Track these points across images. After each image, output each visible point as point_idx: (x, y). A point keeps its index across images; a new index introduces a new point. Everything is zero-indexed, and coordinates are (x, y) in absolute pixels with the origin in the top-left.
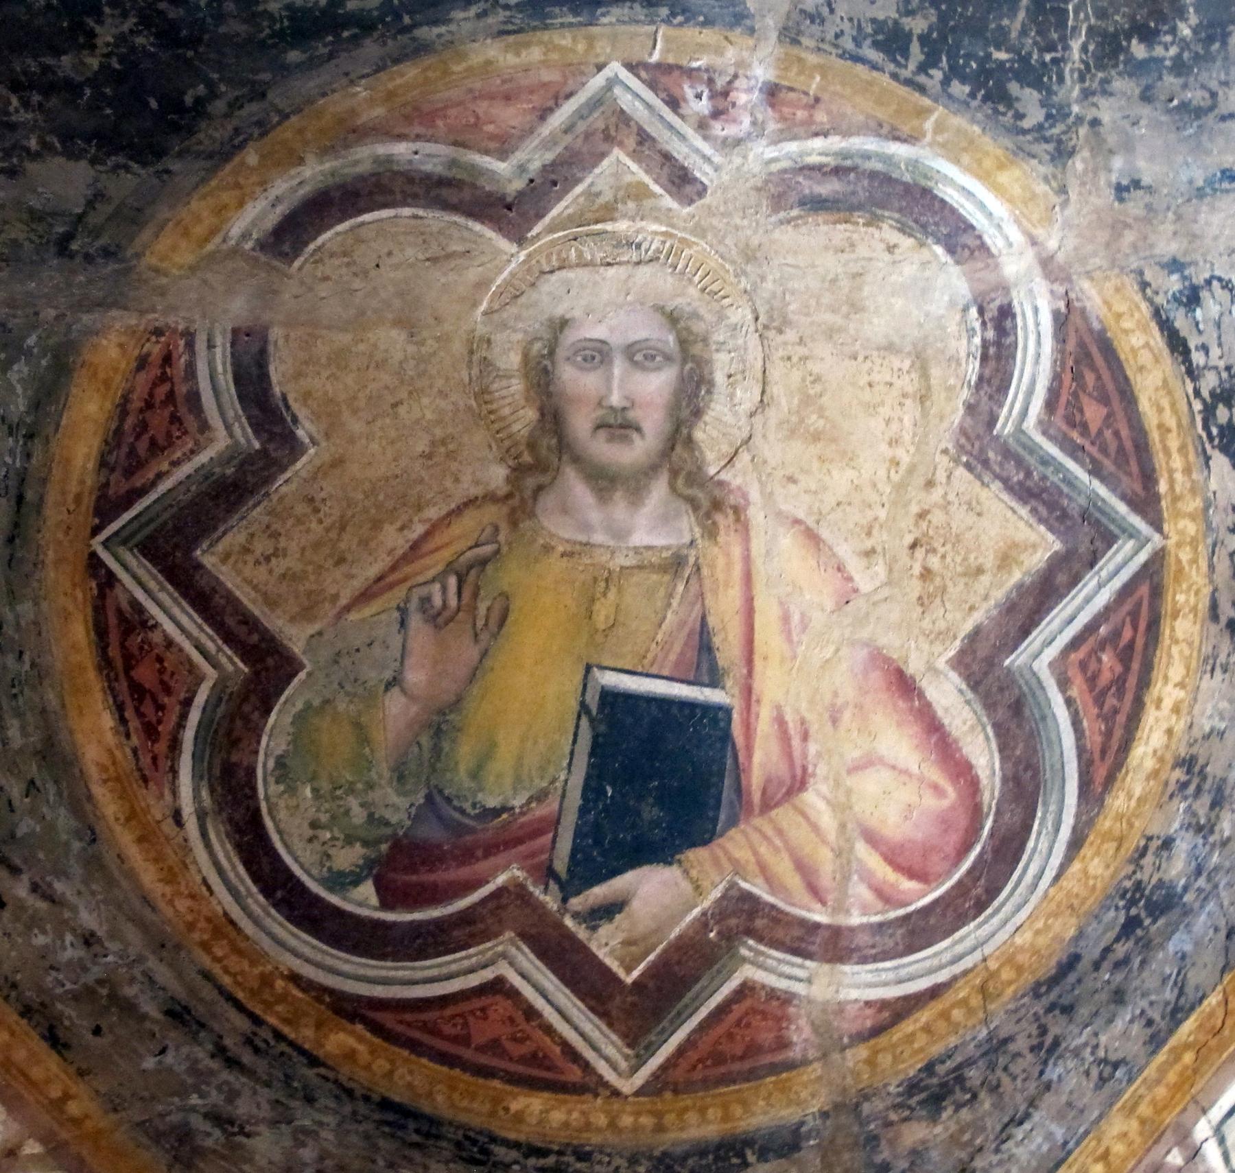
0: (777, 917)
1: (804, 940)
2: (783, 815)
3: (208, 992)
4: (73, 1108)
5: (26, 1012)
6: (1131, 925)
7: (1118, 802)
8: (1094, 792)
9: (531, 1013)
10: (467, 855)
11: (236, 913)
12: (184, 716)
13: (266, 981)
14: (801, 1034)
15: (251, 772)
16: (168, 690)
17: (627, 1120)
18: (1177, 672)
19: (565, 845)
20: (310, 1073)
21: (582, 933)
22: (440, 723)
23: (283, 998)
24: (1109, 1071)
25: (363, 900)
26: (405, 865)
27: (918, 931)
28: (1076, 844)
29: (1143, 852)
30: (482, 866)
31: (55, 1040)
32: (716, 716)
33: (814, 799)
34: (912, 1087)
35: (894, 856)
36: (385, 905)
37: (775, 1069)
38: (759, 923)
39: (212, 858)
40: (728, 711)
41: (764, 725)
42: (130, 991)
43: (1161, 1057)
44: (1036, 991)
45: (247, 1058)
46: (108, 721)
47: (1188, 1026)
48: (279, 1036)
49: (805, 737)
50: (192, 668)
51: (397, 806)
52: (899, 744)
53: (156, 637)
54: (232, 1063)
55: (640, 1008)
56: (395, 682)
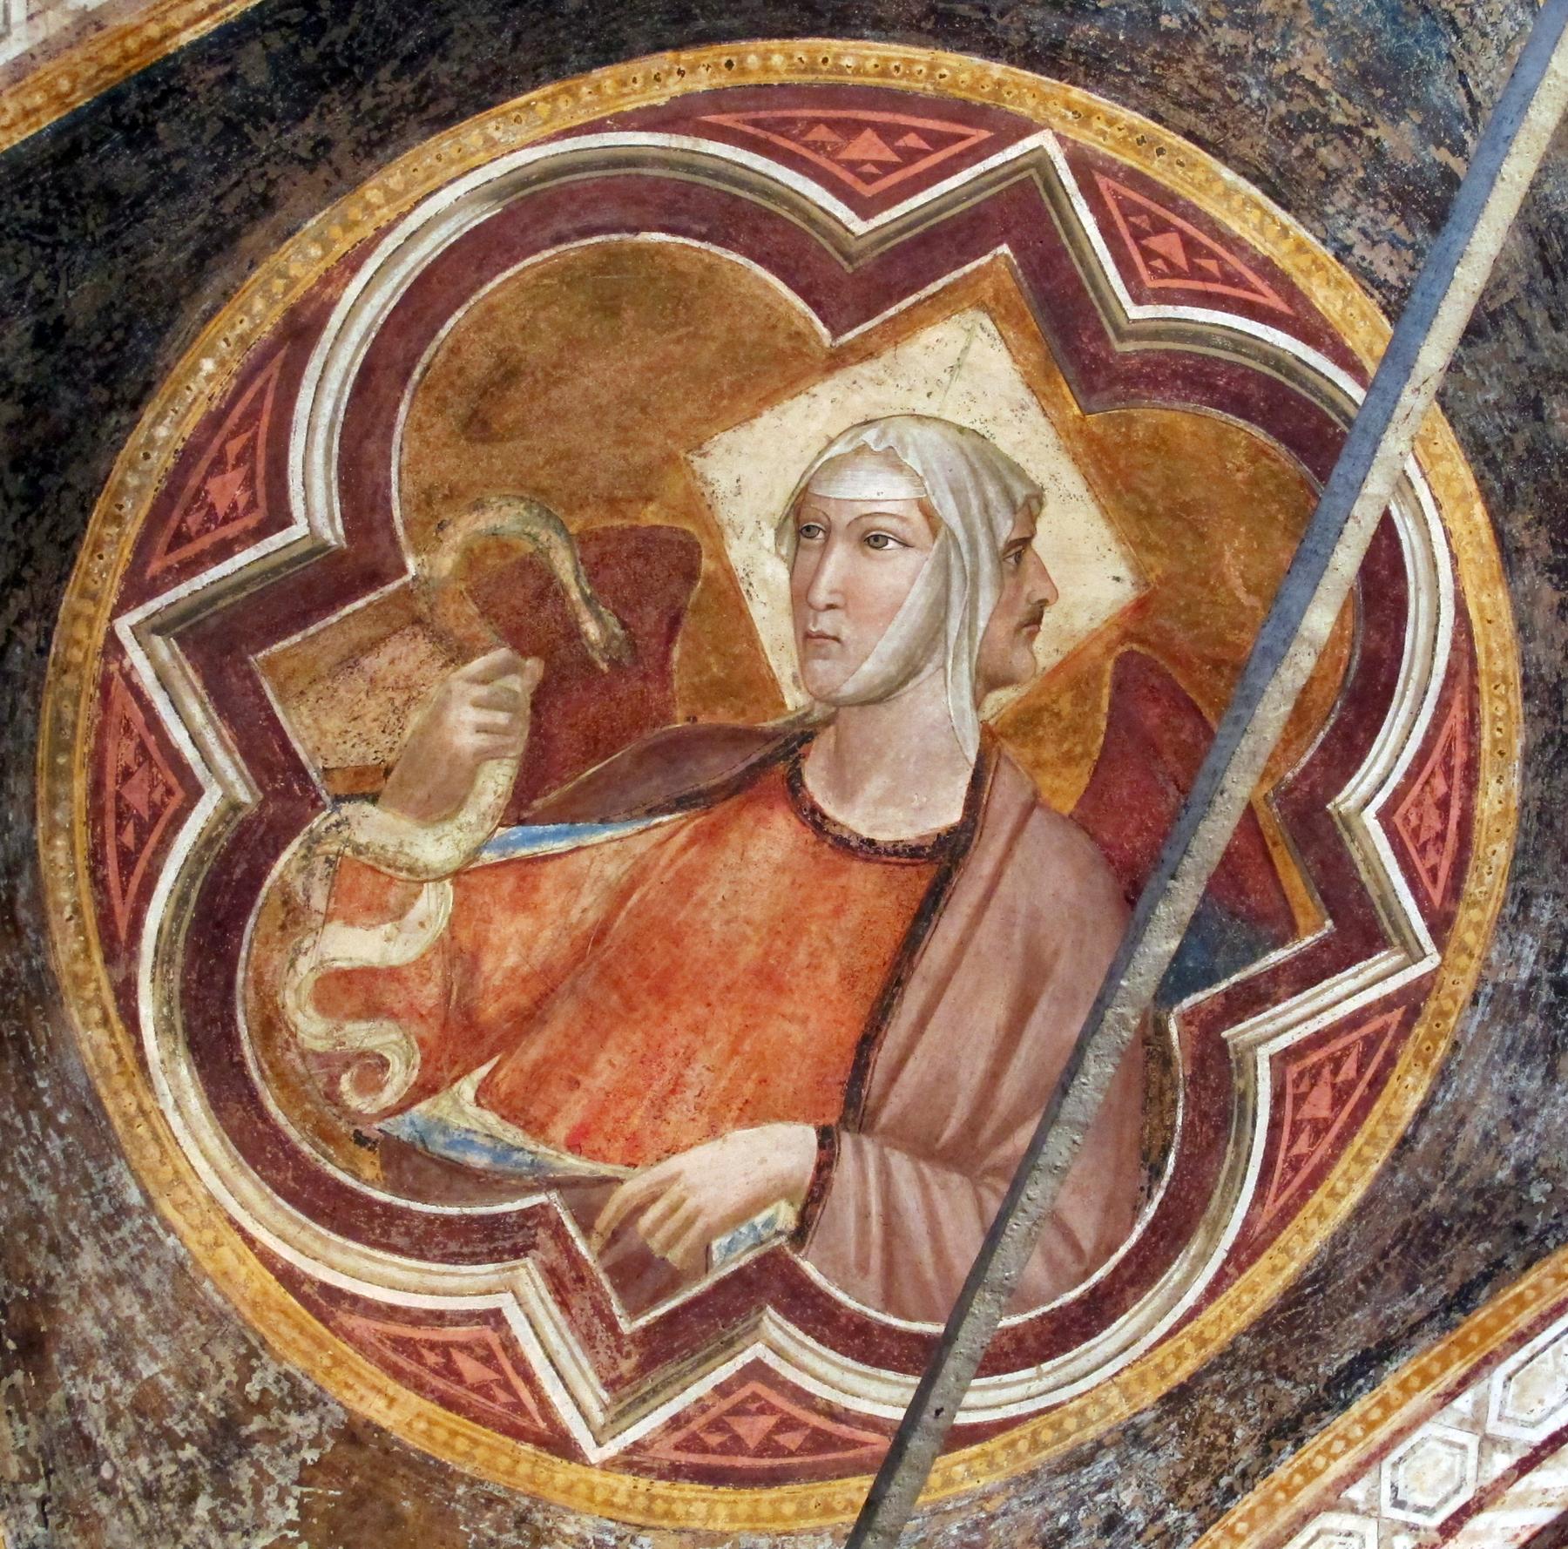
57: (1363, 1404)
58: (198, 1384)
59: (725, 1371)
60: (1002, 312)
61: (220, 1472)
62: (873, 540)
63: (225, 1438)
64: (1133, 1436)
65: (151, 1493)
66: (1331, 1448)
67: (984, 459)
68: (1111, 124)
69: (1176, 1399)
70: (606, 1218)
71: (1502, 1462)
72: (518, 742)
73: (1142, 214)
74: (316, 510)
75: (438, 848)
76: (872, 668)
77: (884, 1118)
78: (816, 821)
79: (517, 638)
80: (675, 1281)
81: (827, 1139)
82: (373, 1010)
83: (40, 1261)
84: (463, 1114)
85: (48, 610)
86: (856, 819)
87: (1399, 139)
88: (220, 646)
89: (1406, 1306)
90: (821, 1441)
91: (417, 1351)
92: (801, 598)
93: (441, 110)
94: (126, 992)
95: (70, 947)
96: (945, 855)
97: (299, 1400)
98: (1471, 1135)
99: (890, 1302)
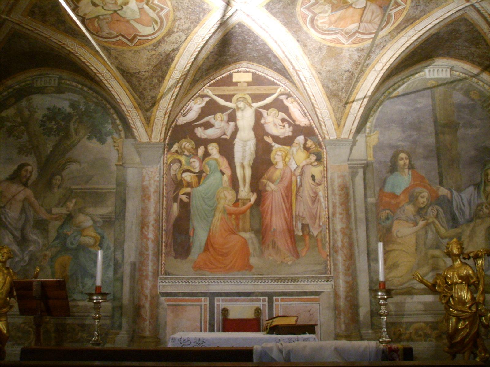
57: (404, 30)
58: (317, 46)
59: (355, 37)
61: (320, 51)
63: (320, 48)
64: (386, 35)
65: (316, 53)
66: (403, 33)
69: (390, 33)
70: (344, 31)
71: (417, 32)
72: (331, 8)
77: (364, 21)
79: (330, 4)
80: (349, 33)
81: (359, 23)
82: (324, 24)
83: (305, 41)
84: (332, 27)
85: (296, 9)
88: (308, 9)
90: (362, 40)
91: (332, 41)
94: (307, 26)
95: (302, 24)
96: (365, 8)
97: (324, 45)
98: (411, 14)
99: (366, 31)
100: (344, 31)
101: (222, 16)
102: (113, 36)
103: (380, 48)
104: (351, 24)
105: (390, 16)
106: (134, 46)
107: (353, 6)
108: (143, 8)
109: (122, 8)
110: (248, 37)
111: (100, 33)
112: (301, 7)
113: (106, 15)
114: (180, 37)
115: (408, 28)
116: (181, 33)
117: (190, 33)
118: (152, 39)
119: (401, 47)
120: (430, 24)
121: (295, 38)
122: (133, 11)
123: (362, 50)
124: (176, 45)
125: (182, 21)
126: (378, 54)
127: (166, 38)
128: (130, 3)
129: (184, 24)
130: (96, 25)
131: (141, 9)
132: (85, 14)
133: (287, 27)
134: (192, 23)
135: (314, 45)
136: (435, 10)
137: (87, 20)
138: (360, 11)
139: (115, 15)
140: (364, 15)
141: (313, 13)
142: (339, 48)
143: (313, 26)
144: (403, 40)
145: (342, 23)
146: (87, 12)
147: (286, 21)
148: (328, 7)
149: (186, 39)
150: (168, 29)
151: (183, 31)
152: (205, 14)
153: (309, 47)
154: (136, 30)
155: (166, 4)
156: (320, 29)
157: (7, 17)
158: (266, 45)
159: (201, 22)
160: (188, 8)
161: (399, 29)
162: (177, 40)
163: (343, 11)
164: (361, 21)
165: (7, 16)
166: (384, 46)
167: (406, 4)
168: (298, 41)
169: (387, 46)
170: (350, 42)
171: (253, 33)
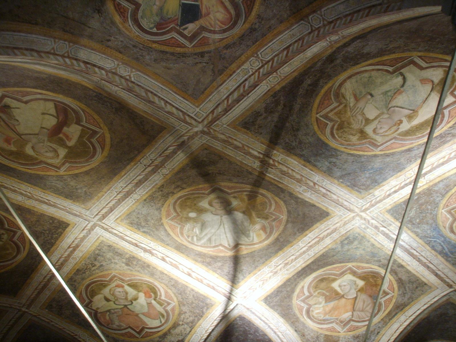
0: (207, 29)
1: (210, 31)
2: (207, 18)
3: (137, 43)
4: (124, 59)
5: (116, 51)
6: (250, 32)
7: (249, 18)
8: (246, 18)
9: (177, 40)
10: (167, 24)
11: (139, 34)
12: (128, 14)
13: (144, 41)
14: (211, 41)
15: (138, 18)
16: (125, 11)
17: (190, 50)
18: (258, 4)
19: (179, 21)
20: (151, 49)
21: (183, 31)
22: (161, 9)
23: (147, 42)
24: (248, 46)
25: (155, 30)
26: (159, 26)
27: (225, 31)
28: (244, 22)
29: (253, 24)
30: (168, 25)
31: (120, 52)
32: (197, 6)
33: (211, 16)
34: (224, 47)
35: (222, 23)
36: (157, 30)
37: (208, 45)
38: (205, 30)
39: (135, 31)
40: (199, 5)
41: (204, 6)
42: (128, 45)
43: (254, 46)
44: (239, 38)
45: (143, 49)
46: (118, 17)
47: (257, 43)
48: (147, 46)
49: (209, 8)
50: (128, 8)
51: (157, 19)
52: (221, 10)
53: (122, 6)
54: (142, 50)
55: (191, 39)
56: (155, 4)
57: (396, 316)
60: (350, 273)
62: (345, 286)
64: (379, 322)
66: (394, 319)
67: (351, 280)
68: (354, 264)
69: (382, 319)
70: (339, 320)
71: (408, 317)
73: (358, 267)
74: (307, 294)
75: (321, 306)
76: (347, 291)
77: (357, 309)
78: (346, 298)
80: (344, 322)
81: (352, 312)
82: (320, 314)
83: (303, 331)
84: (327, 317)
86: (349, 298)
87: (376, 259)
88: (303, 301)
89: (398, 311)
90: (357, 328)
91: (328, 330)
92: (341, 289)
93: (307, 276)
94: (303, 317)
95: (299, 315)
96: (356, 298)
97: (321, 334)
100: (339, 320)
101: (223, 310)
102: (122, 328)
103: (375, 335)
104: (344, 313)
105: (380, 304)
106: (142, 337)
107: (345, 296)
108: (151, 303)
109: (132, 303)
110: (249, 328)
111: (110, 325)
112: (297, 300)
113: (117, 309)
114: (185, 329)
115: (399, 314)
116: (186, 326)
117: (195, 325)
118: (159, 332)
119: (395, 332)
120: (419, 309)
121: (293, 328)
122: (142, 306)
123: (358, 337)
124: (181, 337)
125: (187, 315)
126: (373, 340)
127: (171, 331)
128: (139, 299)
129: (188, 317)
130: (108, 318)
131: (149, 304)
132: (98, 308)
133: (285, 319)
134: (196, 316)
135: (312, 334)
136: (422, 297)
137: (99, 313)
138: (353, 301)
139: (125, 309)
140: (356, 304)
141: (308, 304)
142: (335, 336)
143: (309, 317)
144: (395, 326)
145: (336, 313)
146: (100, 306)
147: (283, 312)
148: (321, 299)
149: (190, 331)
150: (173, 322)
151: (187, 324)
152: (208, 308)
153: (307, 337)
154: (144, 323)
155: (172, 300)
156: (316, 319)
157: (26, 310)
158: (266, 335)
159: (204, 316)
160: (192, 303)
161: (391, 316)
162: (182, 332)
163: (336, 301)
164: (354, 310)
165: (27, 309)
166: (378, 333)
167: (393, 292)
168: (296, 331)
169: (381, 332)
170: (345, 330)
171: (253, 324)
